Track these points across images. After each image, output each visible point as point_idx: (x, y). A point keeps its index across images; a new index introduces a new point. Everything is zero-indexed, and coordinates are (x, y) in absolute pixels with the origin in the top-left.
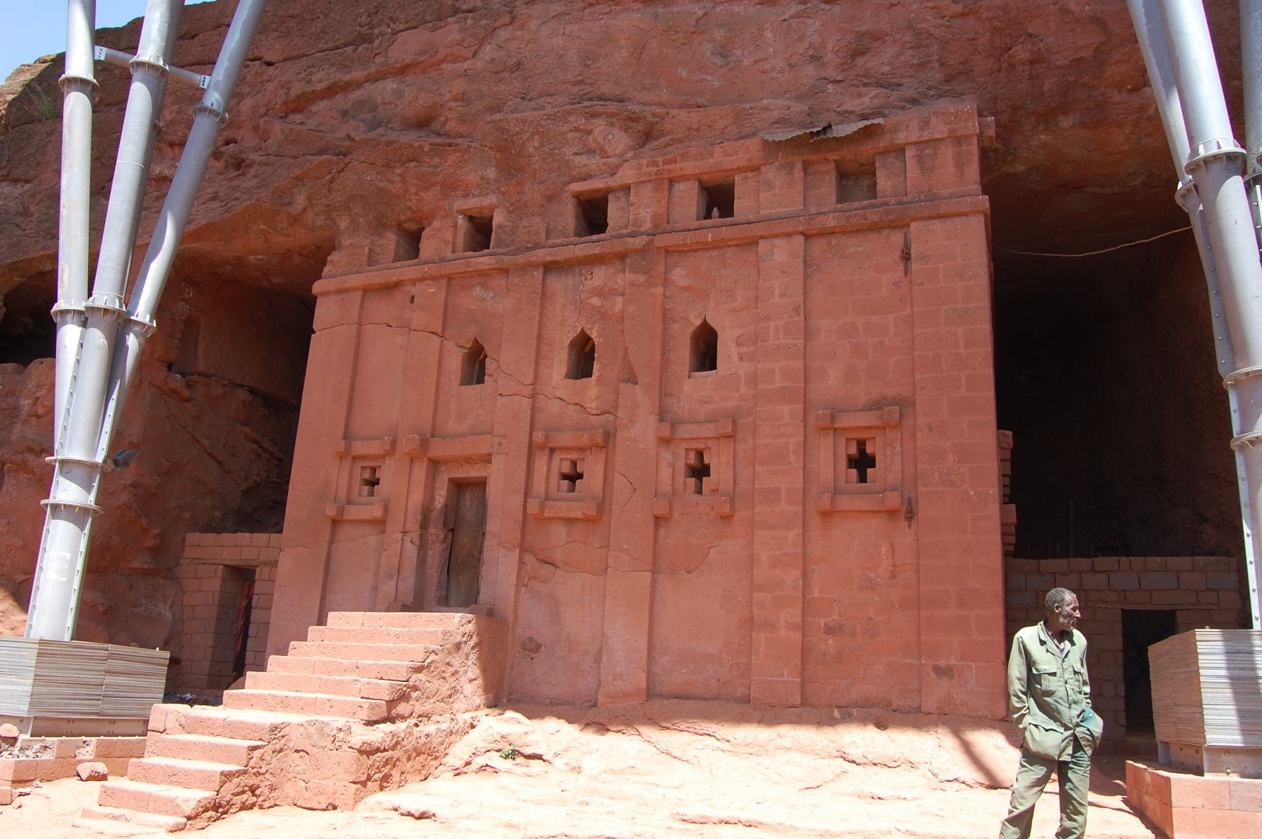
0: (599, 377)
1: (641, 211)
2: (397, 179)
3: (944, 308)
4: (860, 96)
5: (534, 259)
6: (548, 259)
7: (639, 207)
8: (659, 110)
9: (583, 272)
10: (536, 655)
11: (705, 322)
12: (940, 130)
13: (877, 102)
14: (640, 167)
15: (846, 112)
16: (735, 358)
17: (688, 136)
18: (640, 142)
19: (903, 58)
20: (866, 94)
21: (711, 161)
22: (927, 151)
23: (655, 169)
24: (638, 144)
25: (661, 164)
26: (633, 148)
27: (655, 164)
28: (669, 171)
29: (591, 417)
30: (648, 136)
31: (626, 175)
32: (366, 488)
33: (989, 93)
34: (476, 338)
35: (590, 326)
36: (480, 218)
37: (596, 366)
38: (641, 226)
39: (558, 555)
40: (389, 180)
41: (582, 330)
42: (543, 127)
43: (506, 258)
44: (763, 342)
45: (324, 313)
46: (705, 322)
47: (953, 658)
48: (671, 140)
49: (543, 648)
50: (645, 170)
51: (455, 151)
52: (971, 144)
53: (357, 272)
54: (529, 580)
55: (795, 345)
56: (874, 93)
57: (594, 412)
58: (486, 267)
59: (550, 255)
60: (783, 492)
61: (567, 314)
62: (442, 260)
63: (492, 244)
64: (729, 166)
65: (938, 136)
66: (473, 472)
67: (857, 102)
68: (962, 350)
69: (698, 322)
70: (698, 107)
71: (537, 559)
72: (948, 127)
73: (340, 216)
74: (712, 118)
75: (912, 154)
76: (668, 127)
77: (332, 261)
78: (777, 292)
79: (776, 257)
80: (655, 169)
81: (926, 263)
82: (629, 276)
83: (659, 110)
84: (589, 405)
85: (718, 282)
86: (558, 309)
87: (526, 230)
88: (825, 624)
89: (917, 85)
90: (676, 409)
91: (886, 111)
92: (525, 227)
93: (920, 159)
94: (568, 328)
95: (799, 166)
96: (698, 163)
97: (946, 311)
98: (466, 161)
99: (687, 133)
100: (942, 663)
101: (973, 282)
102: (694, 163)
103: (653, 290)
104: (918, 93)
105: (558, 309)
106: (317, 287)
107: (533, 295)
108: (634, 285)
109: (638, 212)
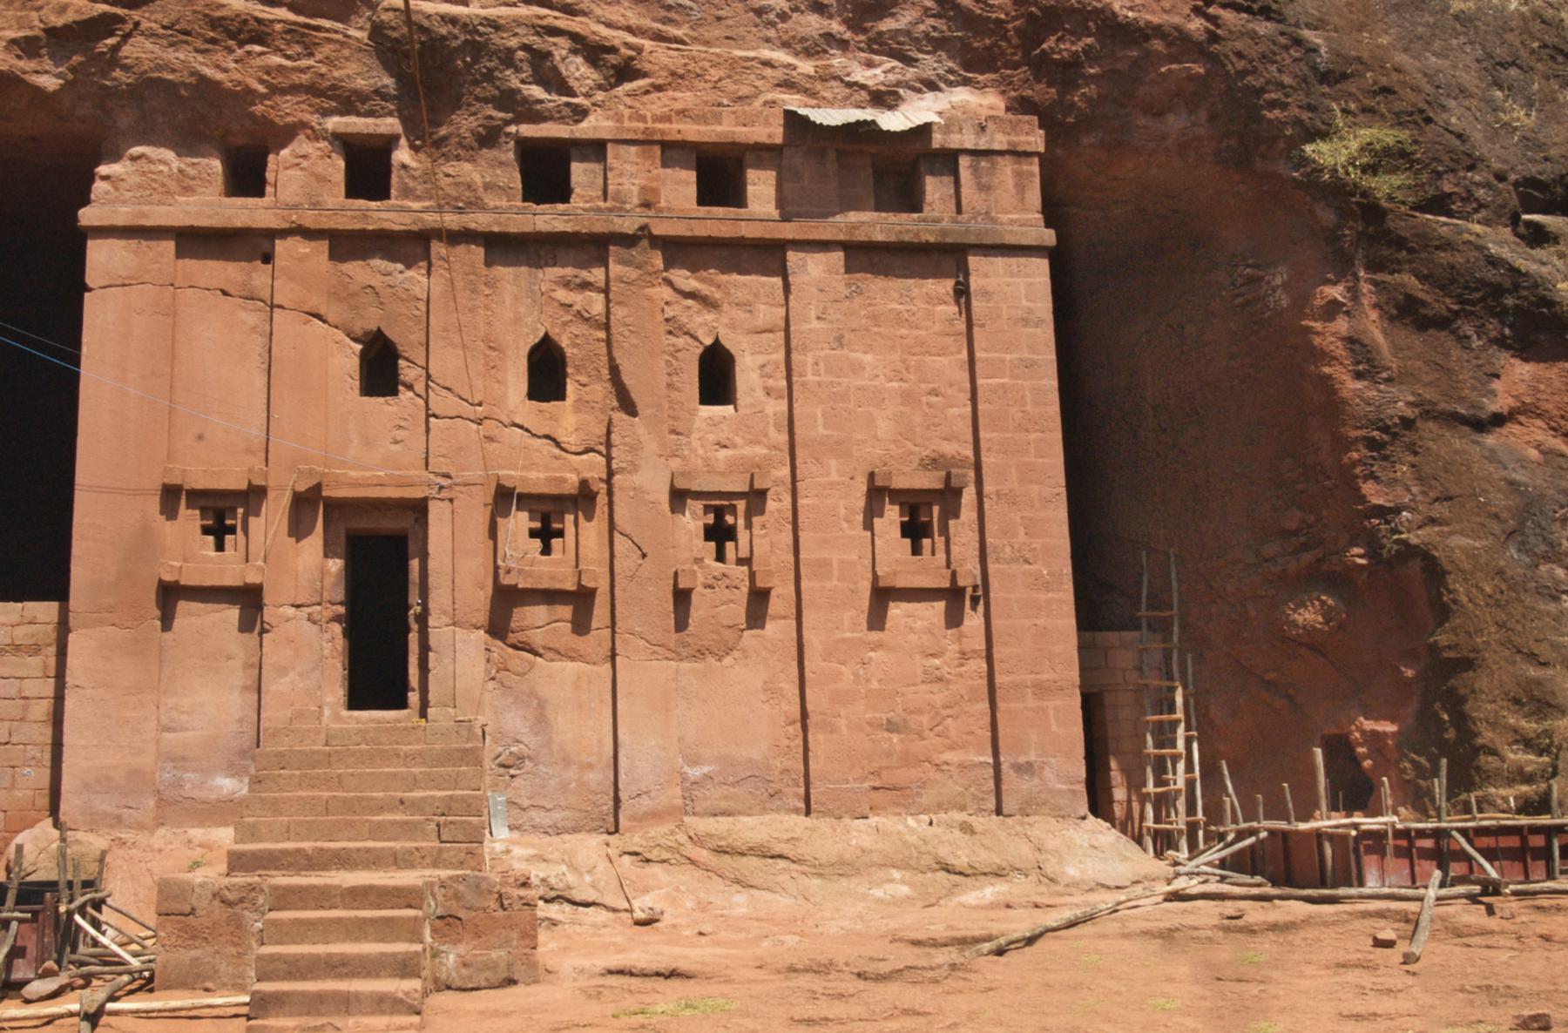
0: (579, 400)
1: (624, 180)
2: (233, 65)
3: (1008, 357)
4: (870, 65)
5: (473, 226)
6: (496, 229)
7: (621, 175)
8: (631, 39)
9: (542, 253)
10: (518, 772)
11: (717, 342)
12: (999, 141)
13: (892, 77)
14: (619, 118)
15: (856, 84)
16: (760, 393)
17: (670, 84)
18: (612, 80)
19: (922, 27)
20: (879, 65)
21: (719, 128)
22: (983, 164)
23: (641, 125)
24: (610, 84)
25: (649, 119)
26: (600, 87)
27: (643, 118)
28: (662, 132)
29: (574, 457)
30: (626, 72)
31: (594, 126)
32: (211, 538)
33: (1015, 90)
35: (557, 331)
37: (571, 387)
38: (624, 202)
39: (537, 638)
40: (218, 67)
42: (481, 35)
43: (426, 216)
44: (801, 376)
45: (101, 258)
46: (717, 342)
47: (1033, 753)
48: (652, 85)
49: (527, 761)
50: (627, 124)
51: (329, 40)
52: (1031, 164)
53: (160, 203)
55: (839, 384)
56: (888, 66)
57: (573, 449)
59: (499, 224)
60: (835, 565)
61: (522, 310)
63: (393, 192)
64: (741, 139)
65: (996, 147)
66: (388, 524)
67: (870, 73)
68: (1029, 408)
69: (709, 341)
70: (677, 42)
72: (1008, 138)
73: (122, 106)
74: (701, 64)
75: (967, 164)
76: (647, 67)
77: (105, 178)
78: (813, 314)
79: (809, 268)
80: (641, 125)
81: (988, 301)
82: (615, 269)
83: (631, 39)
84: (565, 439)
85: (732, 291)
86: (508, 302)
87: (450, 180)
88: (888, 720)
89: (935, 65)
90: (686, 453)
91: (901, 91)
92: (448, 175)
93: (975, 170)
94: (526, 330)
95: (832, 155)
96: (703, 128)
97: (1011, 361)
98: (347, 59)
99: (670, 79)
100: (1022, 760)
101: (1038, 331)
102: (696, 127)
103: (649, 291)
104: (938, 75)
105: (508, 302)
106: (88, 216)
107: (472, 277)
108: (622, 282)
109: (620, 181)
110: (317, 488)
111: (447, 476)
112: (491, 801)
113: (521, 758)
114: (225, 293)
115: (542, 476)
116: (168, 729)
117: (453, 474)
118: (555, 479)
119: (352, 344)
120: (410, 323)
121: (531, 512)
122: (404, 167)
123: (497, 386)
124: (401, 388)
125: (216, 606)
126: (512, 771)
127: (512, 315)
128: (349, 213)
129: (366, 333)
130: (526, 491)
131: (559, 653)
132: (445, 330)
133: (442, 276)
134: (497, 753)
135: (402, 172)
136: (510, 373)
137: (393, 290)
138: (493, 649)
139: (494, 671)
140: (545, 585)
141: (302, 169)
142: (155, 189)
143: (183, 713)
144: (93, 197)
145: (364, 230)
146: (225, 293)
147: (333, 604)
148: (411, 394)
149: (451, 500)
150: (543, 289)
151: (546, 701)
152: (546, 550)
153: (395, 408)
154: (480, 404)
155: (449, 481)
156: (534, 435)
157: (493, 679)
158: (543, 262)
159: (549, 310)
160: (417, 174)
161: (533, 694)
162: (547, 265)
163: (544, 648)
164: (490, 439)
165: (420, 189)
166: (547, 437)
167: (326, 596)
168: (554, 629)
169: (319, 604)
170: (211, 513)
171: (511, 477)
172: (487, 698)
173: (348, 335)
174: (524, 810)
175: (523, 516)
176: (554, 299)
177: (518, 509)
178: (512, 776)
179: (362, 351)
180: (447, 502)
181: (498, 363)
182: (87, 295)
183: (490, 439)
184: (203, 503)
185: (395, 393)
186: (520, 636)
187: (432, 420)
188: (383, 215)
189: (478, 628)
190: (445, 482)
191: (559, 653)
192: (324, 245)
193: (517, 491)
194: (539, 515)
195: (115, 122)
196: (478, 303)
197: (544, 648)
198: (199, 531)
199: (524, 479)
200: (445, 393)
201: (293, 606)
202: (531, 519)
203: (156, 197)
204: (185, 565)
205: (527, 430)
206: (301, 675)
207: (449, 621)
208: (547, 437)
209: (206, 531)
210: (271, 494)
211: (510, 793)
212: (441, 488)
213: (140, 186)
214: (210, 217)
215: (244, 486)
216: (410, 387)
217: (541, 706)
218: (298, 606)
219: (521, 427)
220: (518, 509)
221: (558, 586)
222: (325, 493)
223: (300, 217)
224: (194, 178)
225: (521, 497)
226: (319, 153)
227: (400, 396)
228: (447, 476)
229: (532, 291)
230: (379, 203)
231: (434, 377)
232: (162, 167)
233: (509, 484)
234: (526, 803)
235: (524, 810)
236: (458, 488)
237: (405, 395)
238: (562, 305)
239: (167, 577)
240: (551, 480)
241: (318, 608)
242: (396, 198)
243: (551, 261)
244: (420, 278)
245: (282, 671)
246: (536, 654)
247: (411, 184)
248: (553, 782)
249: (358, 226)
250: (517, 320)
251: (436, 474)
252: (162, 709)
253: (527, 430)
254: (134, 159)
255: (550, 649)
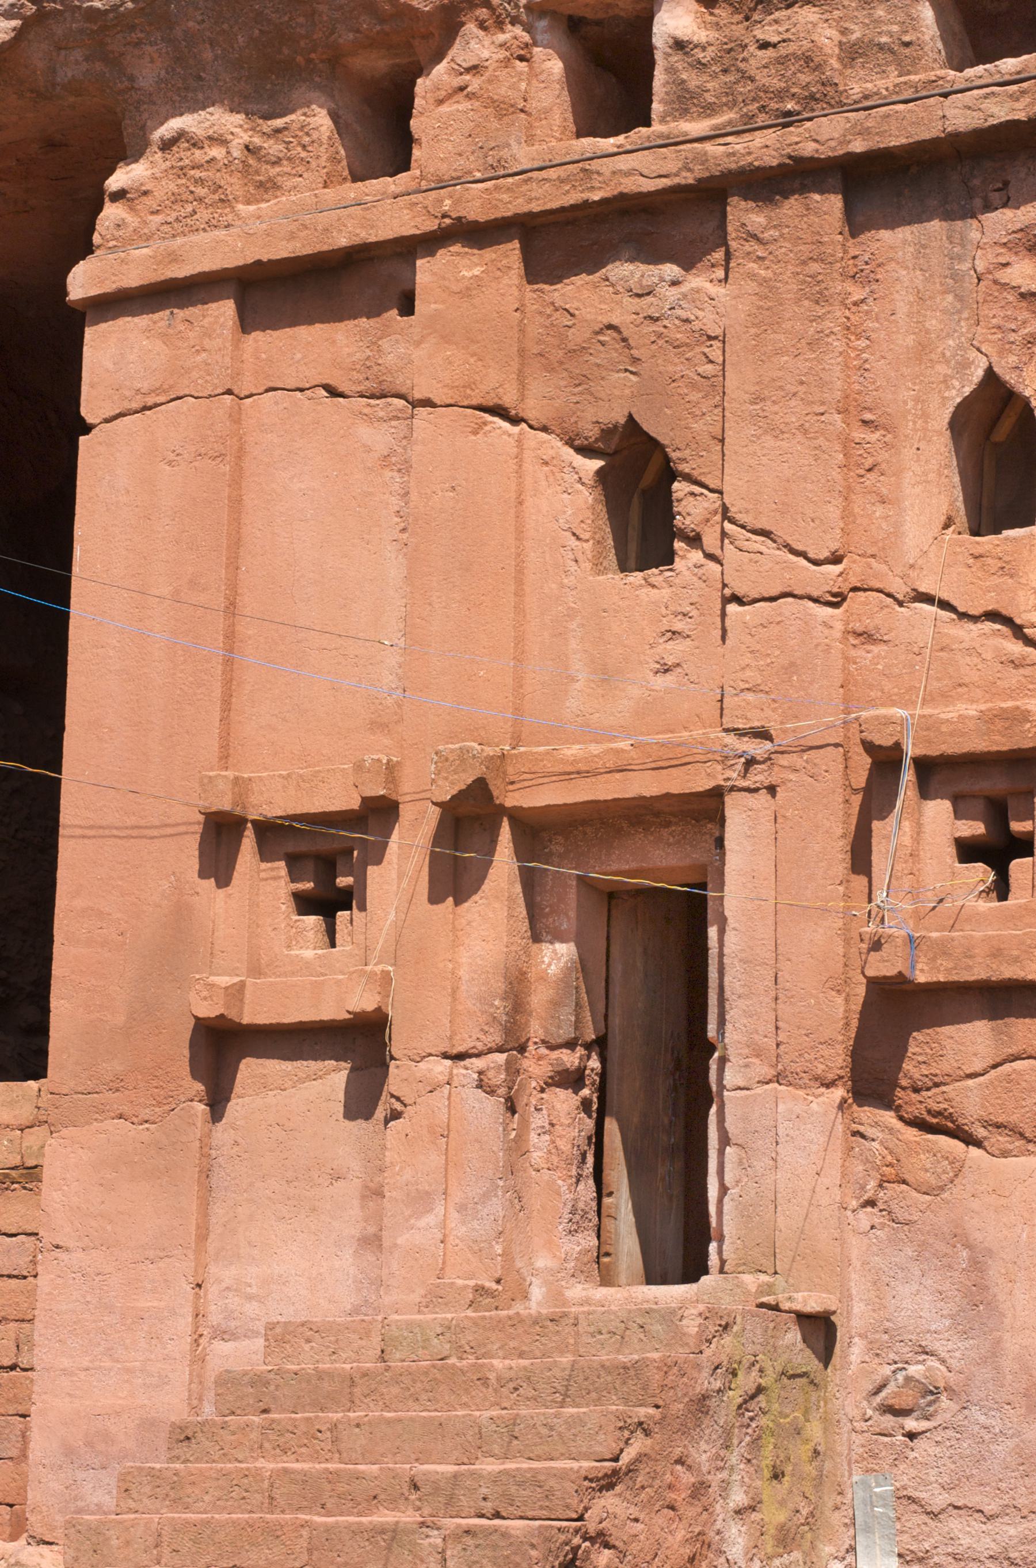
5: (808, 149)
6: (858, 146)
9: (976, 182)
10: (924, 1425)
32: (312, 921)
34: (631, 418)
36: (598, 23)
41: (990, 374)
49: (944, 1401)
54: (880, 1186)
58: (649, 186)
59: (865, 133)
61: (932, 324)
62: (497, 172)
63: (657, 107)
71: (901, 1118)
73: (138, 44)
77: (119, 195)
86: (902, 309)
87: (770, 53)
92: (764, 45)
94: (942, 369)
105: (902, 309)
107: (815, 267)
110: (480, 789)
111: (763, 734)
112: (860, 1494)
113: (932, 1392)
114: (333, 392)
115: (972, 711)
116: (223, 1334)
117: (774, 728)
118: (1003, 715)
119: (579, 460)
120: (695, 396)
121: (957, 800)
122: (679, 45)
123: (879, 511)
124: (678, 545)
125: (313, 1065)
126: (911, 1424)
127: (910, 340)
128: (552, 173)
129: (607, 433)
130: (933, 751)
131: (1022, 1135)
132: (757, 399)
133: (752, 276)
134: (878, 1380)
135: (676, 58)
136: (908, 477)
137: (657, 327)
138: (869, 1132)
139: (872, 1184)
140: (978, 973)
141: (470, 97)
142: (200, 200)
143: (250, 1298)
144: (96, 239)
145: (586, 204)
146: (333, 392)
147: (552, 1048)
148: (697, 556)
149: (772, 790)
150: (980, 269)
151: (990, 1252)
152: (1002, 889)
153: (666, 592)
154: (836, 559)
155: (768, 745)
156: (963, 616)
157: (871, 1203)
158: (978, 202)
159: (995, 314)
160: (704, 56)
161: (959, 1237)
162: (989, 207)
163: (986, 1124)
164: (867, 637)
165: (713, 86)
166: (993, 616)
167: (535, 1030)
168: (1008, 1078)
169: (500, 1050)
170: (310, 866)
171: (889, 721)
172: (856, 1247)
173: (570, 443)
174: (934, 1515)
175: (939, 809)
176: (1004, 286)
177: (925, 792)
178: (911, 1436)
179: (600, 473)
180: (763, 796)
181: (883, 456)
182: (82, 439)
183: (867, 637)
184: (291, 847)
185: (667, 558)
186: (933, 1100)
187: (732, 608)
188: (624, 163)
189: (828, 1085)
190: (757, 748)
191: (1022, 1135)
192: (511, 252)
193: (910, 750)
194: (980, 806)
195: (132, 79)
196: (828, 324)
197: (986, 1124)
198: (286, 906)
199: (928, 724)
200: (758, 543)
201: (446, 1056)
202: (958, 815)
203: (204, 214)
204: (250, 981)
205: (945, 605)
206: (461, 1208)
207: (767, 1071)
208: (993, 616)
209: (305, 904)
210: (406, 813)
211: (904, 1477)
212: (750, 762)
213: (177, 200)
214: (292, 236)
215: (355, 804)
216: (695, 540)
217: (977, 1265)
218: (460, 1057)
219: (927, 599)
220: (925, 792)
221: (1009, 972)
222: (511, 800)
223: (456, 203)
224: (277, 162)
225: (925, 767)
226: (503, 54)
227: (678, 564)
228: (763, 734)
229: (956, 277)
230: (621, 139)
231: (733, 511)
232: (217, 152)
233: (884, 739)
234: (939, 1500)
235: (934, 1515)
236: (784, 760)
237: (687, 558)
238: (1023, 295)
239: (207, 1010)
240: (989, 718)
241: (501, 1058)
242: (663, 120)
243: (995, 197)
244: (713, 290)
245: (422, 1201)
246: (970, 1140)
247: (693, 79)
248: (1002, 1448)
249: (574, 198)
250: (923, 350)
251: (740, 733)
252: (212, 1290)
253: (945, 605)
254: (167, 145)
255: (998, 1126)
